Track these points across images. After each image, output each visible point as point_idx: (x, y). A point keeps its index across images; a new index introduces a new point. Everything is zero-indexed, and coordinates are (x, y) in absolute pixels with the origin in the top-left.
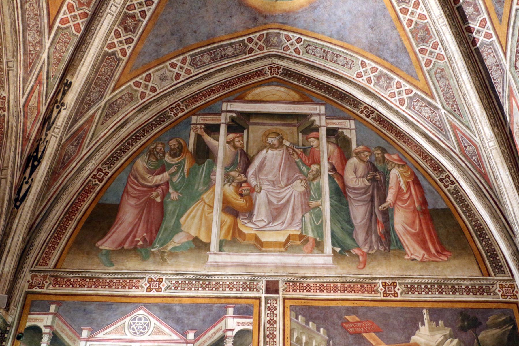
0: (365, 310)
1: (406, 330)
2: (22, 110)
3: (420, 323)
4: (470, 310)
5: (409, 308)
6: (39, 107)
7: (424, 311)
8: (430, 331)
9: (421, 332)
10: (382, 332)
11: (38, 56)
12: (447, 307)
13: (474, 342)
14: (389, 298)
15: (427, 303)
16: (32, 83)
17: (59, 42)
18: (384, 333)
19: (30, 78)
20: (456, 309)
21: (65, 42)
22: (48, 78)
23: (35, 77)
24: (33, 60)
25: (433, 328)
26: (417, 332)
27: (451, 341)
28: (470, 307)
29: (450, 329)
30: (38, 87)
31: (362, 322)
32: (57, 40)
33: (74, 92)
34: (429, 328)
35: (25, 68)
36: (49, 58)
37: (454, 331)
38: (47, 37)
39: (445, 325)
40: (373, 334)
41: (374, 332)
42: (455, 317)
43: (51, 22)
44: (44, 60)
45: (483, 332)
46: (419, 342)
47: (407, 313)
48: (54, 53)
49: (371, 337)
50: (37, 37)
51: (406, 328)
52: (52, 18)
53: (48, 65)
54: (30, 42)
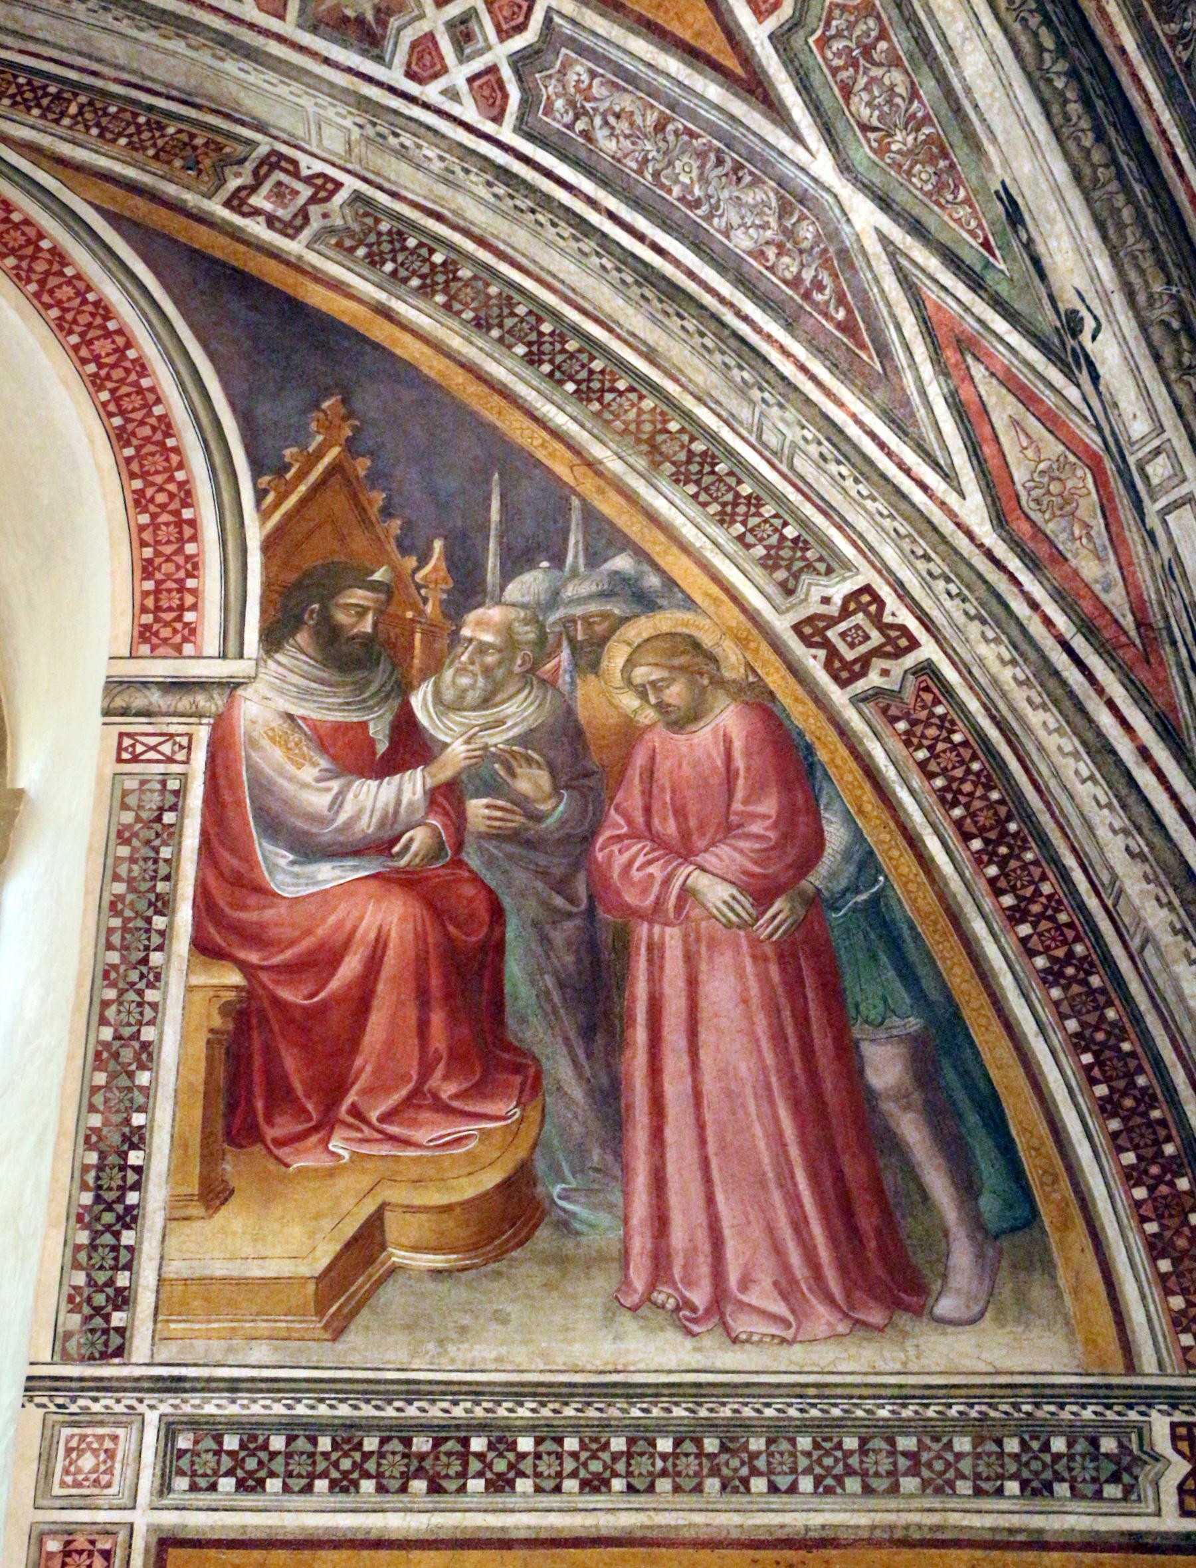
2: (1001, 550)
6: (1071, 443)
11: (843, 253)
16: (935, 392)
17: (847, 91)
19: (909, 379)
21: (867, 51)
22: (976, 283)
23: (921, 352)
24: (841, 301)
30: (978, 371)
32: (830, 96)
33: (1052, 207)
35: (848, 370)
36: (884, 203)
38: (785, 143)
43: (732, 63)
44: (884, 240)
48: (882, 150)
50: (760, 196)
52: (715, 46)
53: (917, 229)
54: (760, 255)
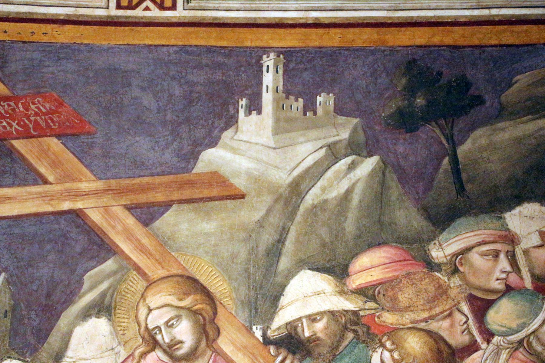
0: (37, 56)
1: (184, 129)
3: (243, 102)
4: (446, 53)
5: (210, 49)
7: (269, 61)
8: (276, 132)
9: (240, 136)
10: (89, 133)
12: (359, 44)
13: (439, 165)
14: (139, 13)
15: (281, 31)
18: (99, 139)
20: (393, 50)
25: (289, 120)
26: (227, 135)
27: (352, 167)
28: (448, 40)
29: (355, 121)
31: (16, 99)
34: (277, 120)
37: (367, 127)
39: (339, 110)
40: (54, 143)
41: (58, 136)
42: (383, 80)
45: (478, 132)
46: (225, 171)
47: (199, 67)
49: (44, 153)
51: (188, 121)
